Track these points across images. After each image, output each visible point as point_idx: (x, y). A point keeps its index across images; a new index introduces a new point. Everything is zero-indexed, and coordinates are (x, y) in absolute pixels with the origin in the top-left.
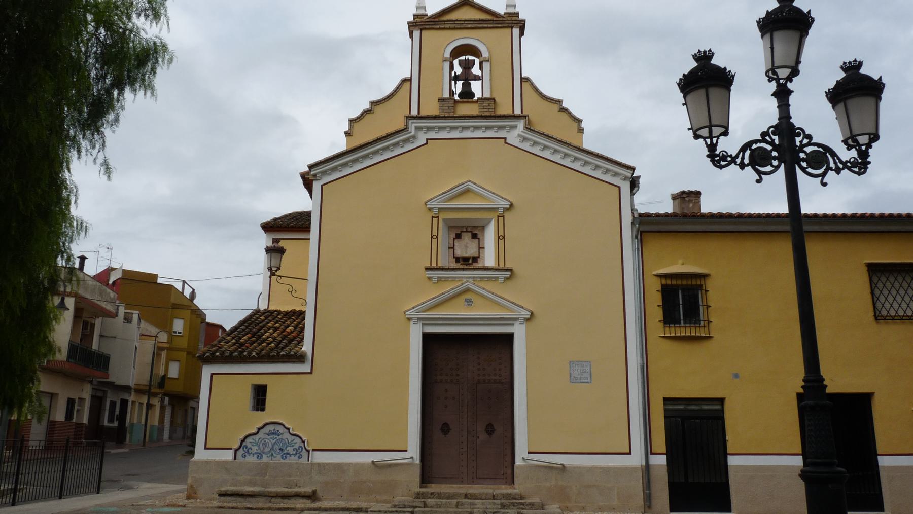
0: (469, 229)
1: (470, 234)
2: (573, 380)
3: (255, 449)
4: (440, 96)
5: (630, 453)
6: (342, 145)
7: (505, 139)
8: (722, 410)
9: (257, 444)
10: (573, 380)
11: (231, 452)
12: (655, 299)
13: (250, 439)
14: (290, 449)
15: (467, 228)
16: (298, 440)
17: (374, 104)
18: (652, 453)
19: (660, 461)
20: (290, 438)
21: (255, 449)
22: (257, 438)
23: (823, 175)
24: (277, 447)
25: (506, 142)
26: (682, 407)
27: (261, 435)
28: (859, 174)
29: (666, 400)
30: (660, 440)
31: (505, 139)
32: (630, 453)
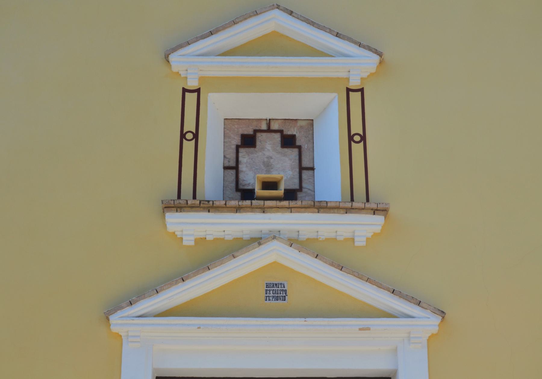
0: (275, 126)
1: (277, 137)
15: (269, 122)
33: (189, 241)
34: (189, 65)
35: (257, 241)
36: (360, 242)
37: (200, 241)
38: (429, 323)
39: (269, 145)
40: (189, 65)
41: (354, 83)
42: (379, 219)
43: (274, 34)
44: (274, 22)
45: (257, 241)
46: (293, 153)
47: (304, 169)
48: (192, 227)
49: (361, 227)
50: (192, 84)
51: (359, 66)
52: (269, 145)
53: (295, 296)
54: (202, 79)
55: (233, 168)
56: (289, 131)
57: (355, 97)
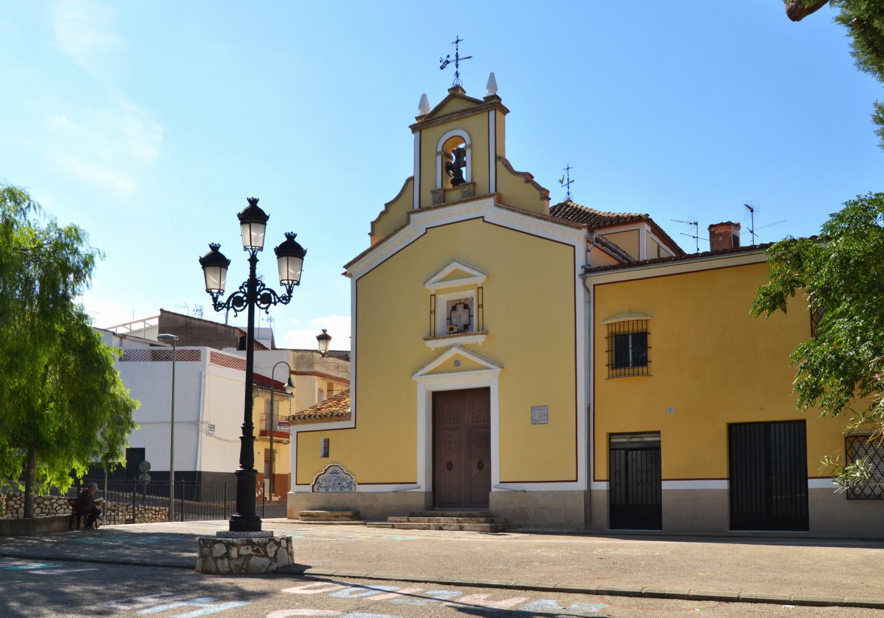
2: (534, 422)
3: (324, 484)
4: (433, 189)
5: (576, 481)
6: (367, 244)
7: (483, 217)
8: (660, 441)
9: (325, 480)
10: (534, 422)
11: (310, 487)
12: (603, 345)
13: (321, 477)
14: (344, 484)
16: (349, 477)
17: (387, 205)
18: (595, 480)
19: (602, 487)
20: (345, 476)
21: (324, 484)
22: (325, 476)
23: (267, 308)
24: (337, 482)
25: (484, 221)
26: (625, 440)
27: (327, 474)
28: (286, 303)
29: (611, 435)
30: (602, 471)
31: (483, 217)
32: (576, 481)
33: (433, 349)
34: (431, 287)
35: (450, 347)
36: (480, 344)
37: (436, 349)
38: (497, 371)
39: (460, 308)
40: (431, 287)
41: (480, 285)
42: (484, 336)
43: (457, 270)
44: (455, 266)
45: (450, 347)
46: (467, 311)
47: (470, 316)
48: (433, 344)
49: (479, 339)
50: (433, 293)
51: (480, 279)
52: (460, 308)
53: (463, 365)
54: (436, 291)
55: (449, 319)
56: (467, 302)
57: (480, 290)
